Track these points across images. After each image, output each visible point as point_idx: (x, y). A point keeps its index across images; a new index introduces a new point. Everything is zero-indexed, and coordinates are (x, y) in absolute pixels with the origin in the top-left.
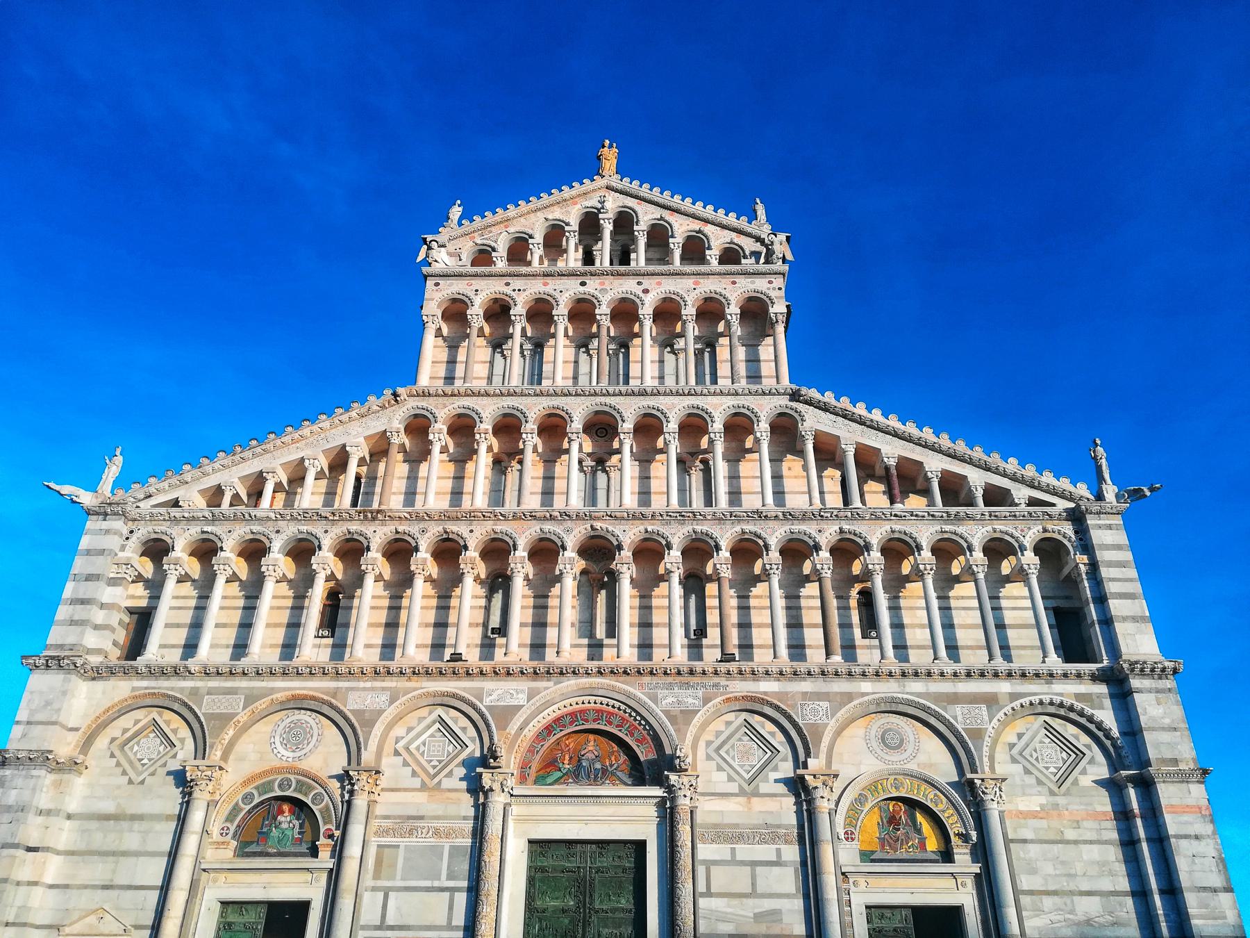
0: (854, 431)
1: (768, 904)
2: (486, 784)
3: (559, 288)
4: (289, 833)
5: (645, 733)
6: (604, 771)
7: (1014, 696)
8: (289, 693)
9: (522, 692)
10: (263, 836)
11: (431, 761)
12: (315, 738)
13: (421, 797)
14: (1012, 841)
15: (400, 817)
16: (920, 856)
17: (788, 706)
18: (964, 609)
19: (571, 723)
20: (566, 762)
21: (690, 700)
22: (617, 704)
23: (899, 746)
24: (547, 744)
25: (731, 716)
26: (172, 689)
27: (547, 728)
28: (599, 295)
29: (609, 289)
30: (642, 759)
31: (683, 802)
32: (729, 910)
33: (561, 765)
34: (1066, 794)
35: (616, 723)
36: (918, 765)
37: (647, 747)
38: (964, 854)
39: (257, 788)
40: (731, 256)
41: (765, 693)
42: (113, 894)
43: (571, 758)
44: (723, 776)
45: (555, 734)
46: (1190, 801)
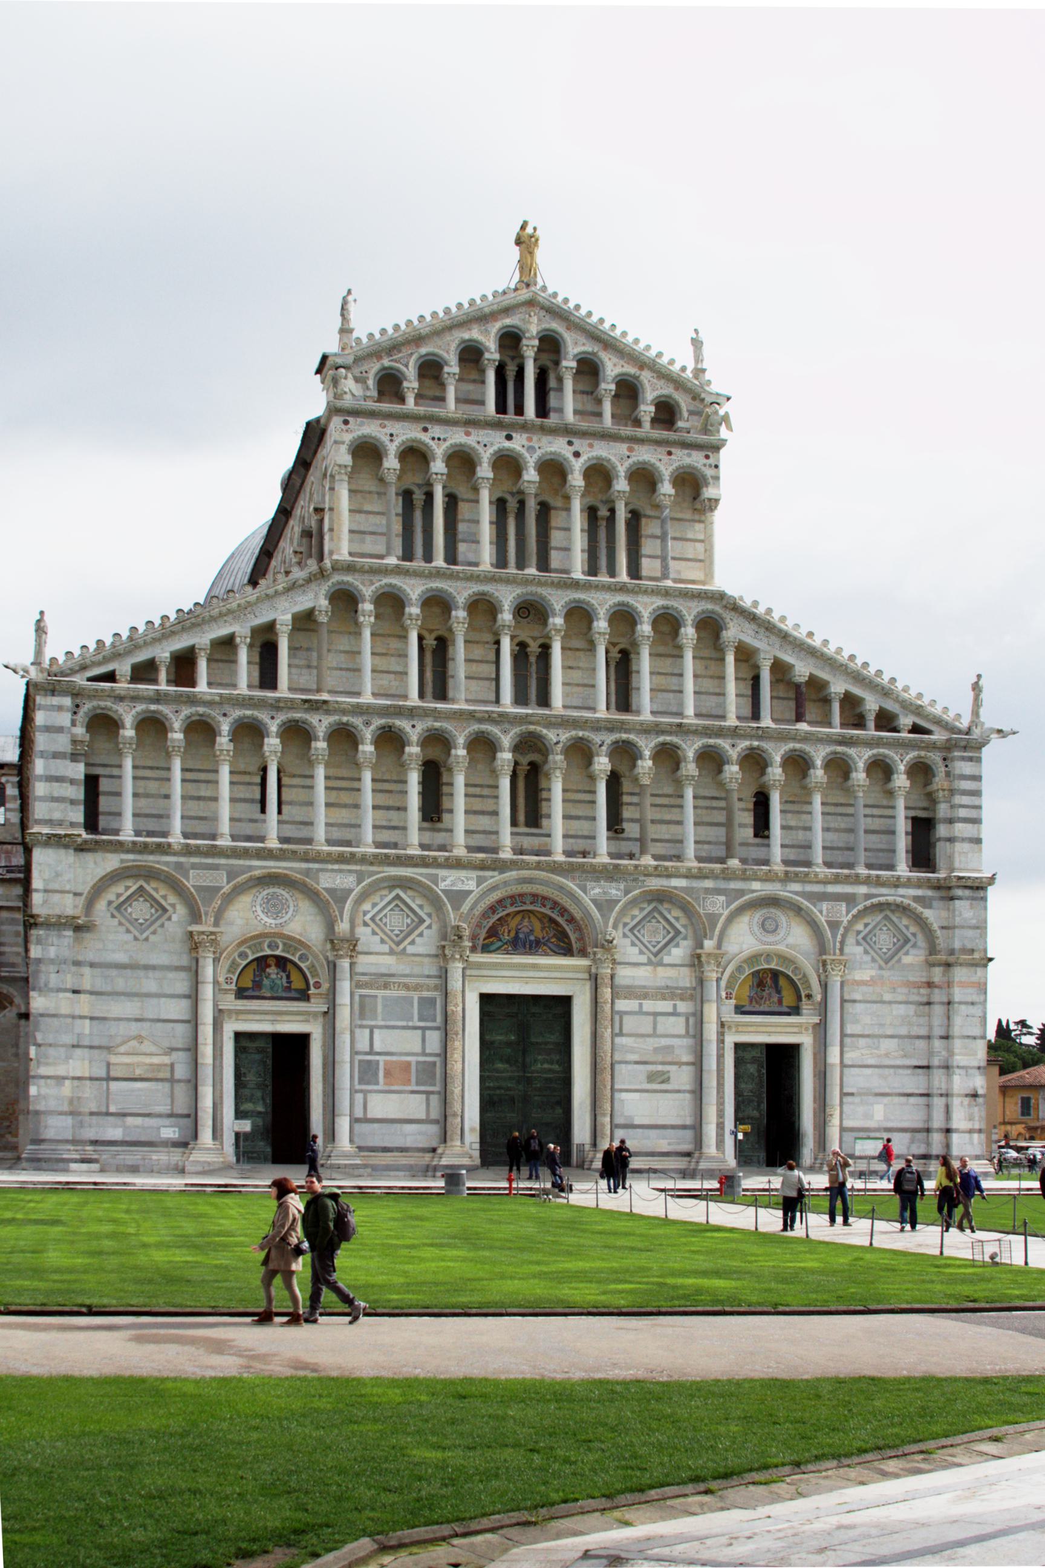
4: (278, 982)
7: (868, 896)
10: (257, 985)
11: (392, 931)
12: (292, 909)
13: (390, 960)
15: (375, 974)
18: (841, 815)
19: (512, 905)
21: (614, 892)
25: (645, 905)
36: (787, 946)
39: (249, 947)
41: (675, 888)
42: (147, 1025)
43: (509, 931)
44: (636, 950)
46: (974, 979)
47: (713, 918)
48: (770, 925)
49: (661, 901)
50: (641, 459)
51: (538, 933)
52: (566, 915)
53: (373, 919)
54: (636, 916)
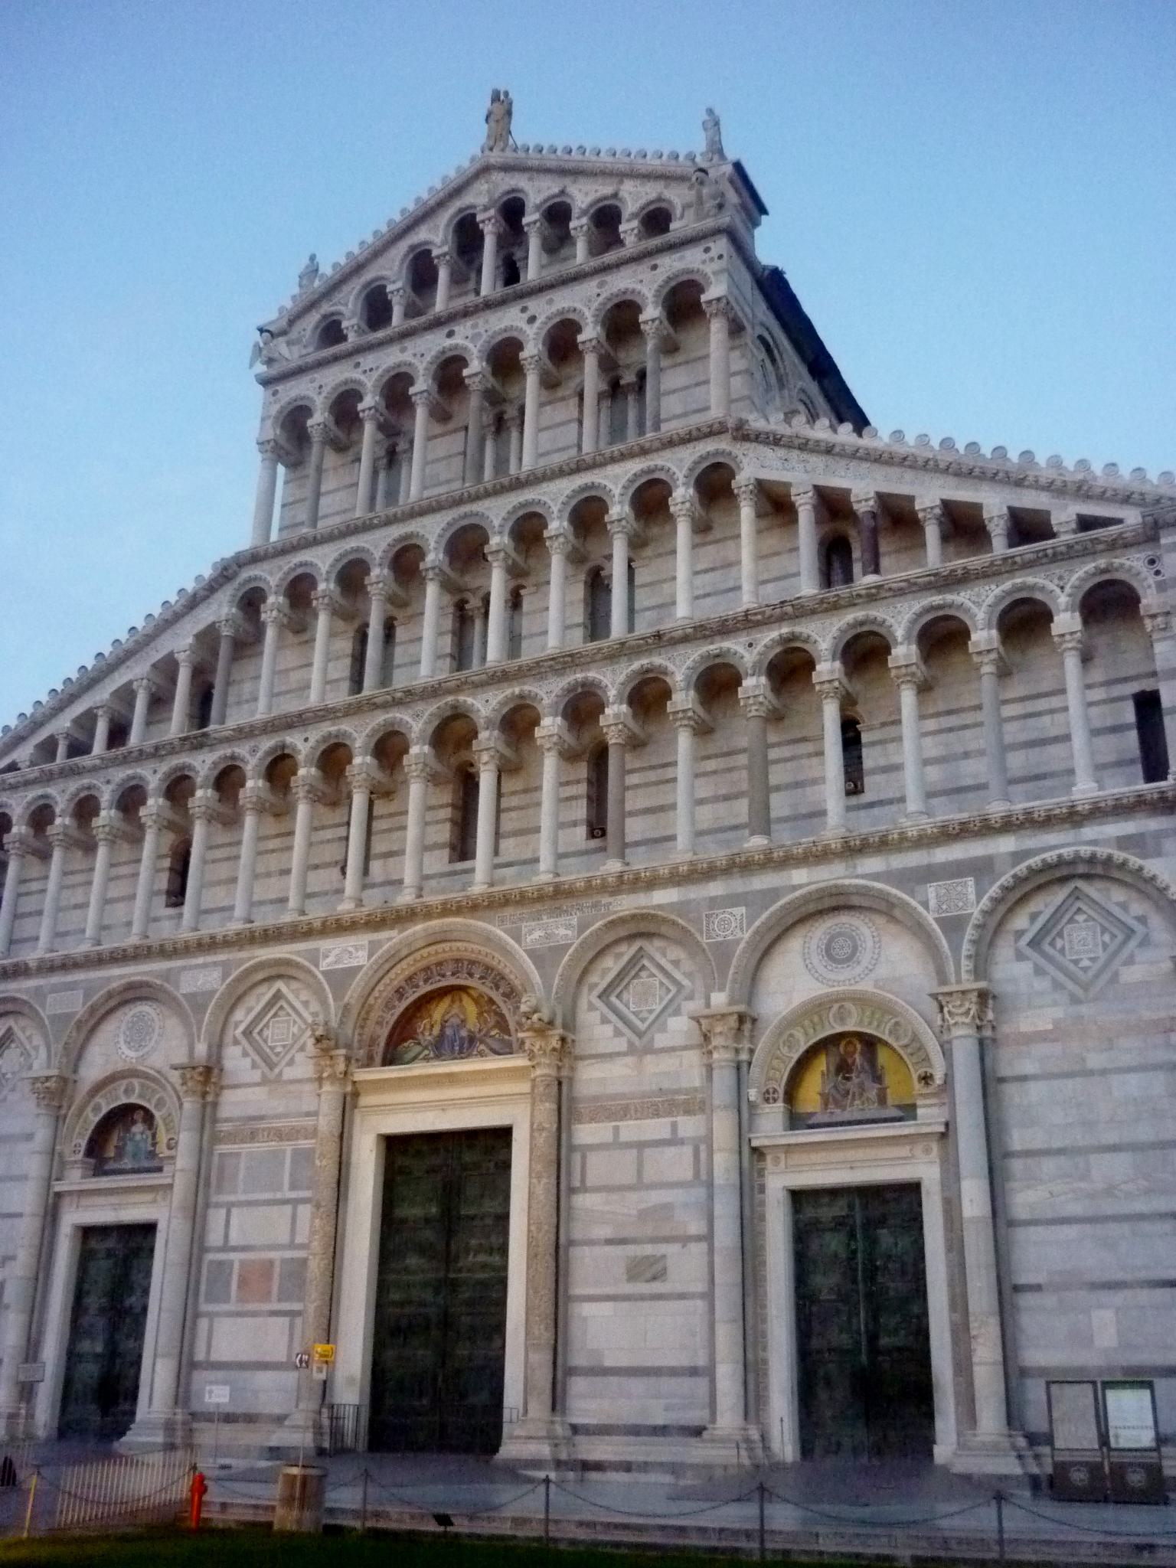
0: (814, 470)
1: (656, 1197)
3: (419, 350)
4: (142, 1145)
6: (472, 1040)
7: (1018, 856)
8: (123, 981)
10: (120, 1153)
13: (260, 1093)
14: (1002, 1080)
15: (239, 1119)
16: (873, 1112)
17: (689, 921)
19: (426, 981)
21: (562, 931)
23: (850, 959)
25: (623, 948)
26: (19, 991)
27: (397, 991)
28: (470, 346)
29: (483, 331)
32: (607, 1208)
34: (1096, 999)
38: (932, 1105)
40: (656, 220)
41: (660, 907)
44: (608, 1030)
47: (723, 951)
48: (842, 949)
49: (648, 935)
50: (615, 290)
51: (473, 1024)
52: (502, 983)
53: (248, 1033)
54: (609, 969)
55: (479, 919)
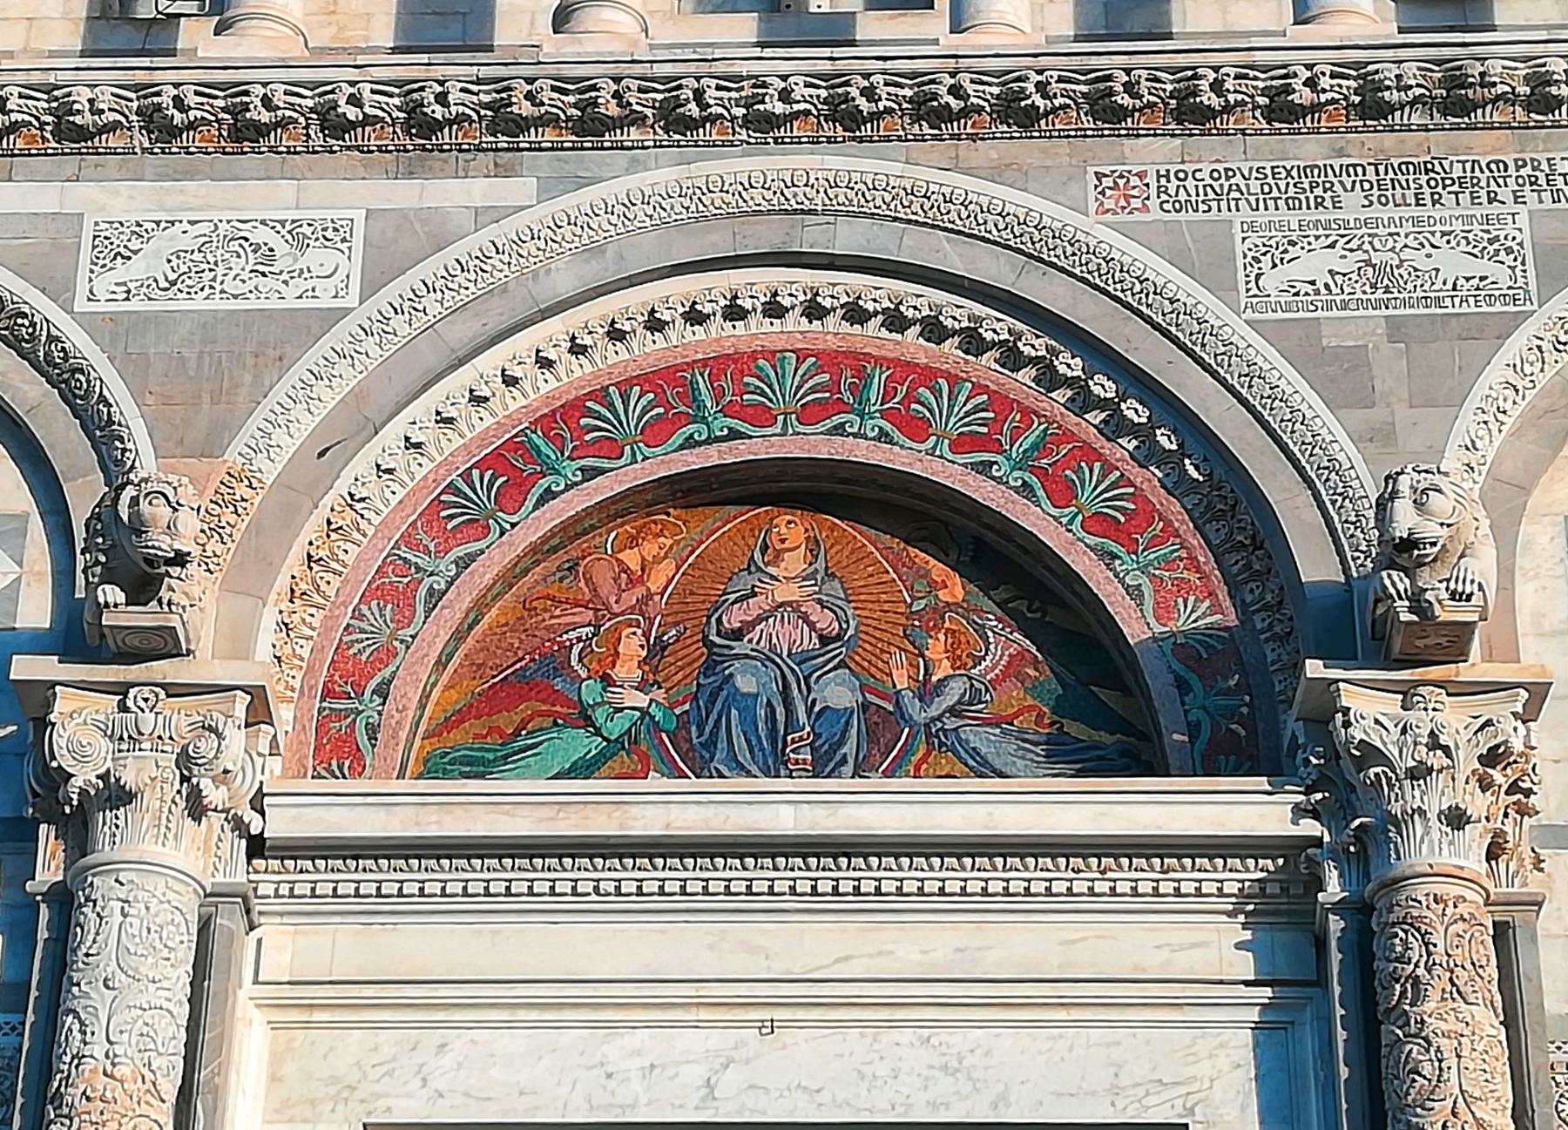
2: (82, 759)
5: (1149, 479)
9: (333, 235)
19: (656, 432)
20: (627, 671)
21: (1453, 264)
22: (957, 310)
24: (498, 554)
27: (495, 461)
30: (1136, 626)
31: (1446, 859)
33: (590, 691)
35: (955, 427)
37: (1169, 564)
43: (656, 650)
45: (548, 495)
55: (995, 174)
